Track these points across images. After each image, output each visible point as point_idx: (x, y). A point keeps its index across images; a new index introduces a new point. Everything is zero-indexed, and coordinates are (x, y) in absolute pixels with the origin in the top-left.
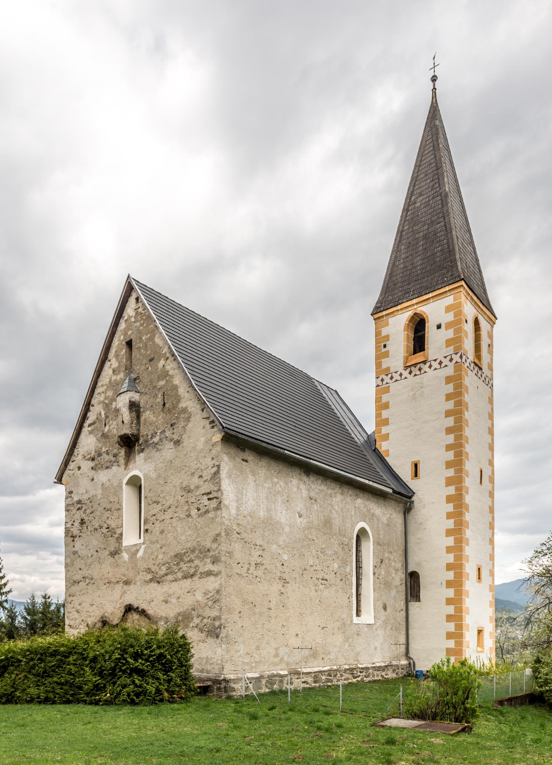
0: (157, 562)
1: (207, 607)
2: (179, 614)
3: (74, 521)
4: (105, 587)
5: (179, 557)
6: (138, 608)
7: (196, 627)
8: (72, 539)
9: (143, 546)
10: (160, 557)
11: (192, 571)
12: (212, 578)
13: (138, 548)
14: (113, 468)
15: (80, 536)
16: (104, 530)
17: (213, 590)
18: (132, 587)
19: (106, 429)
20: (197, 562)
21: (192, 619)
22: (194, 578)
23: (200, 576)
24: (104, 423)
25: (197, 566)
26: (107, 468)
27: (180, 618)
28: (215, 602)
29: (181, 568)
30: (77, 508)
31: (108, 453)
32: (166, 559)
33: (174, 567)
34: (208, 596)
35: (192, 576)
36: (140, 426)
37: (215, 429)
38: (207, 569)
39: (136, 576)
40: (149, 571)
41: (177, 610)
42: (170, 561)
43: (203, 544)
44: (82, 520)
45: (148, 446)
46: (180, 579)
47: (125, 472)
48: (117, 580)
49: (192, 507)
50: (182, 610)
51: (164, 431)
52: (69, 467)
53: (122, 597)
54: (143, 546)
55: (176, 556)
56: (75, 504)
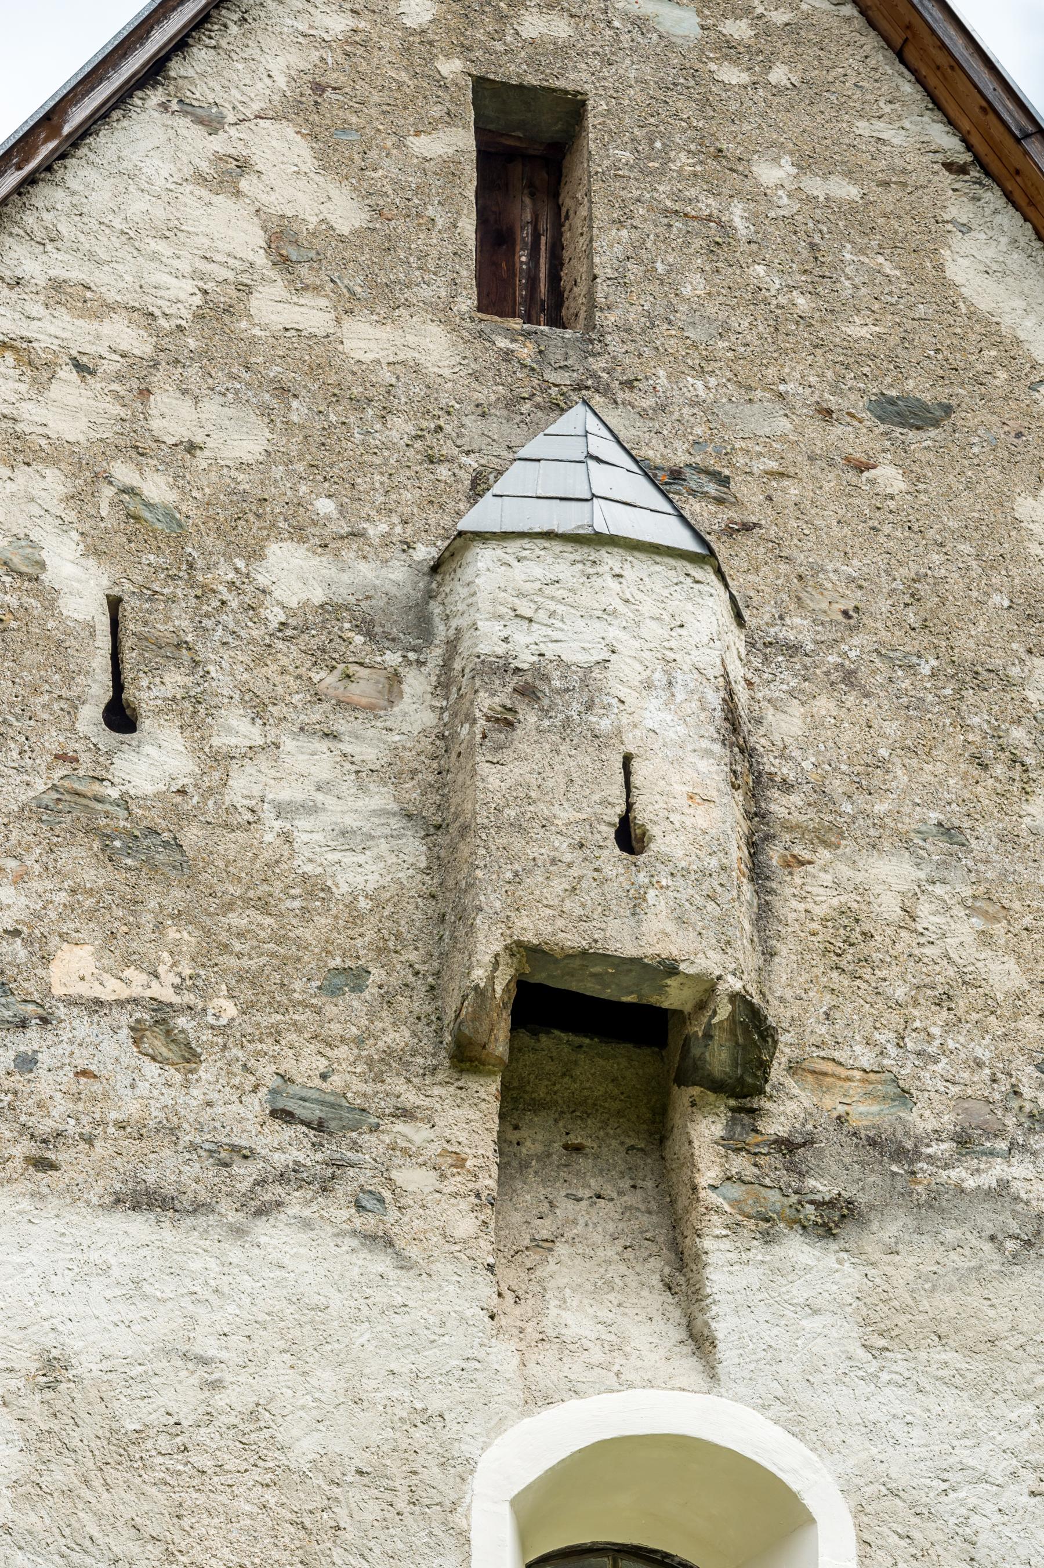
14: (273, 1236)
24: (100, 691)
36: (770, 954)
45: (935, 1205)
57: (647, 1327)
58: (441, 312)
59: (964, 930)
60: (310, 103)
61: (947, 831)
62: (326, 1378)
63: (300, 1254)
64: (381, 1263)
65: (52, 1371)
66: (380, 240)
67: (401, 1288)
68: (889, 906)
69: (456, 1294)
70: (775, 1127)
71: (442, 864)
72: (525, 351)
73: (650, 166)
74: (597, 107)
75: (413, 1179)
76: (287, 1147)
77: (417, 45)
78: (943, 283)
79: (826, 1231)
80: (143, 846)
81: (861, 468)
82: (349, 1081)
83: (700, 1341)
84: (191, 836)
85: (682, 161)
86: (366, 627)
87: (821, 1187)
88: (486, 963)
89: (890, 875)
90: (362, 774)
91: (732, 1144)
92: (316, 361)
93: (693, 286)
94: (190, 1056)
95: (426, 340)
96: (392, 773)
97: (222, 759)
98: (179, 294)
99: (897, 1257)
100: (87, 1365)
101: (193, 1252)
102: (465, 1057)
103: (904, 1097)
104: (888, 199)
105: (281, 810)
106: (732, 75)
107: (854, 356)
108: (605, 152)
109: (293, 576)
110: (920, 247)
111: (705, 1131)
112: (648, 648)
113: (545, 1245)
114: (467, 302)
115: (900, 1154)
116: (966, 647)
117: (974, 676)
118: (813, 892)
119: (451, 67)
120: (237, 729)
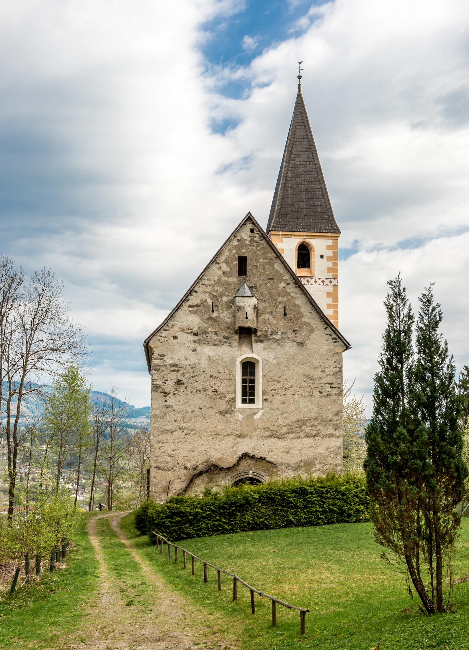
0: (277, 423)
1: (329, 458)
2: (301, 462)
3: (167, 380)
4: (211, 437)
5: (301, 423)
6: (254, 455)
7: (319, 470)
8: (164, 394)
9: (261, 411)
10: (281, 420)
11: (315, 433)
12: (333, 439)
13: (256, 411)
15: (175, 394)
16: (210, 393)
17: (335, 446)
18: (246, 440)
19: (215, 315)
20: (319, 427)
21: (315, 465)
22: (317, 438)
23: (322, 436)
25: (319, 430)
26: (215, 345)
27: (302, 464)
28: (336, 454)
29: (303, 430)
30: (171, 370)
31: (216, 333)
32: (286, 422)
33: (296, 428)
34: (330, 450)
35: (315, 436)
37: (337, 343)
38: (329, 433)
39: (252, 432)
40: (268, 429)
41: (298, 459)
42: (291, 424)
43: (325, 415)
44: (178, 381)
46: (303, 438)
47: (239, 352)
48: (227, 433)
49: (315, 390)
50: (304, 458)
51: (285, 333)
52: (159, 334)
53: (235, 447)
54: (261, 411)
55: (298, 421)
56: (168, 367)
57: (249, 350)
58: (235, 276)
59: (272, 319)
60: (226, 261)
61: (271, 312)
62: (227, 355)
63: (225, 348)
64: (231, 348)
65: (209, 357)
66: (231, 272)
67: (232, 349)
68: (267, 318)
69: (235, 349)
70: (258, 335)
71: (235, 319)
72: (242, 279)
73: (252, 261)
74: (248, 257)
75: (233, 341)
76: (225, 340)
77: (234, 254)
78: (274, 268)
79: (261, 342)
80: (215, 321)
81: (266, 284)
82: (228, 335)
83: (252, 350)
84: (218, 319)
85: (254, 261)
86: (230, 303)
87: (261, 339)
88: (237, 327)
89: (267, 316)
90: (230, 313)
91: (255, 337)
92: (226, 281)
93: (255, 271)
94: (218, 335)
95: (234, 279)
96: (232, 313)
97: (220, 313)
98: (216, 278)
99: (266, 343)
100: (211, 356)
101: (218, 348)
102: (236, 333)
103: (267, 332)
104: (270, 261)
105: (224, 317)
106: (258, 252)
107: (267, 275)
108: (248, 261)
109: (225, 299)
110: (272, 266)
111: (253, 336)
112: (248, 303)
113: (242, 344)
114: (237, 275)
115: (267, 336)
116: (274, 297)
117: (274, 300)
118: (261, 318)
119: (236, 256)
120: (221, 311)
